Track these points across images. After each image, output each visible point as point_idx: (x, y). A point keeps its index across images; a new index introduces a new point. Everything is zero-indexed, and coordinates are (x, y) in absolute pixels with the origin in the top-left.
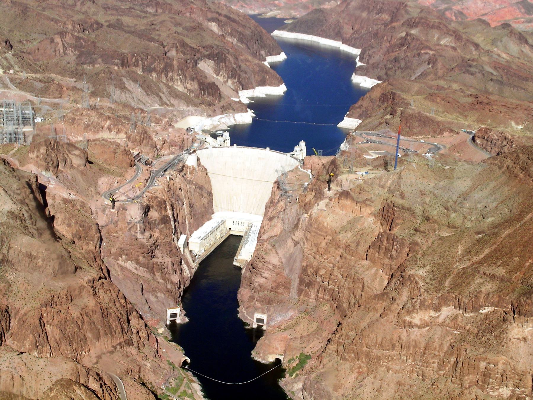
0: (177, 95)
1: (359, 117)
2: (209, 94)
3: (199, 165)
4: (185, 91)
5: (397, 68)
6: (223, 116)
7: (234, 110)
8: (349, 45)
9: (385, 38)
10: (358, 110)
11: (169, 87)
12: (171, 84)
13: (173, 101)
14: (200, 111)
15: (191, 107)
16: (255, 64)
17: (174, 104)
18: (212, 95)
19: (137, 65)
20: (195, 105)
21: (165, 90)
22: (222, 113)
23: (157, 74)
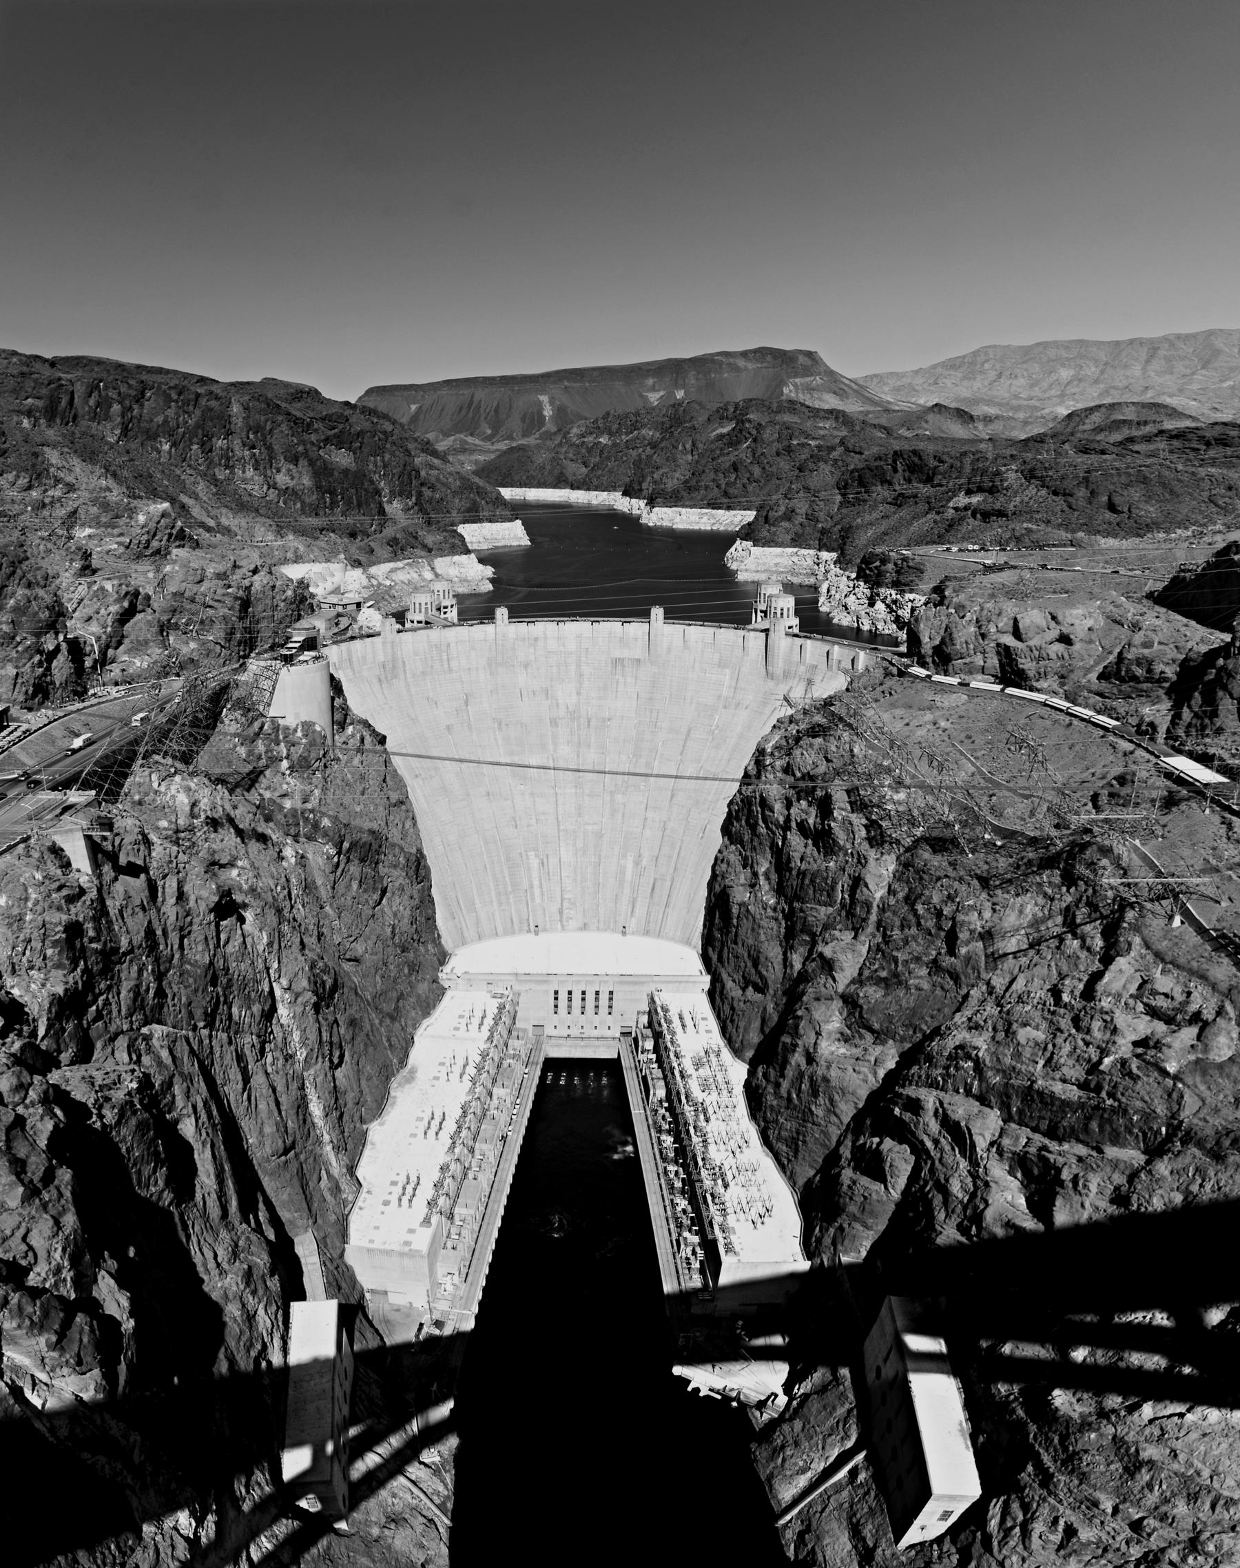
0: (242, 506)
1: (797, 541)
2: (349, 503)
3: (341, 716)
4: (272, 494)
5: (745, 481)
6: (400, 564)
7: (430, 551)
8: (588, 489)
9: (680, 448)
10: (785, 524)
11: (215, 482)
12: (221, 474)
13: (228, 519)
14: (321, 549)
15: (291, 537)
16: (450, 474)
17: (233, 528)
18: (359, 505)
19: (100, 413)
20: (302, 532)
21: (201, 487)
22: (394, 557)
23: (174, 445)
